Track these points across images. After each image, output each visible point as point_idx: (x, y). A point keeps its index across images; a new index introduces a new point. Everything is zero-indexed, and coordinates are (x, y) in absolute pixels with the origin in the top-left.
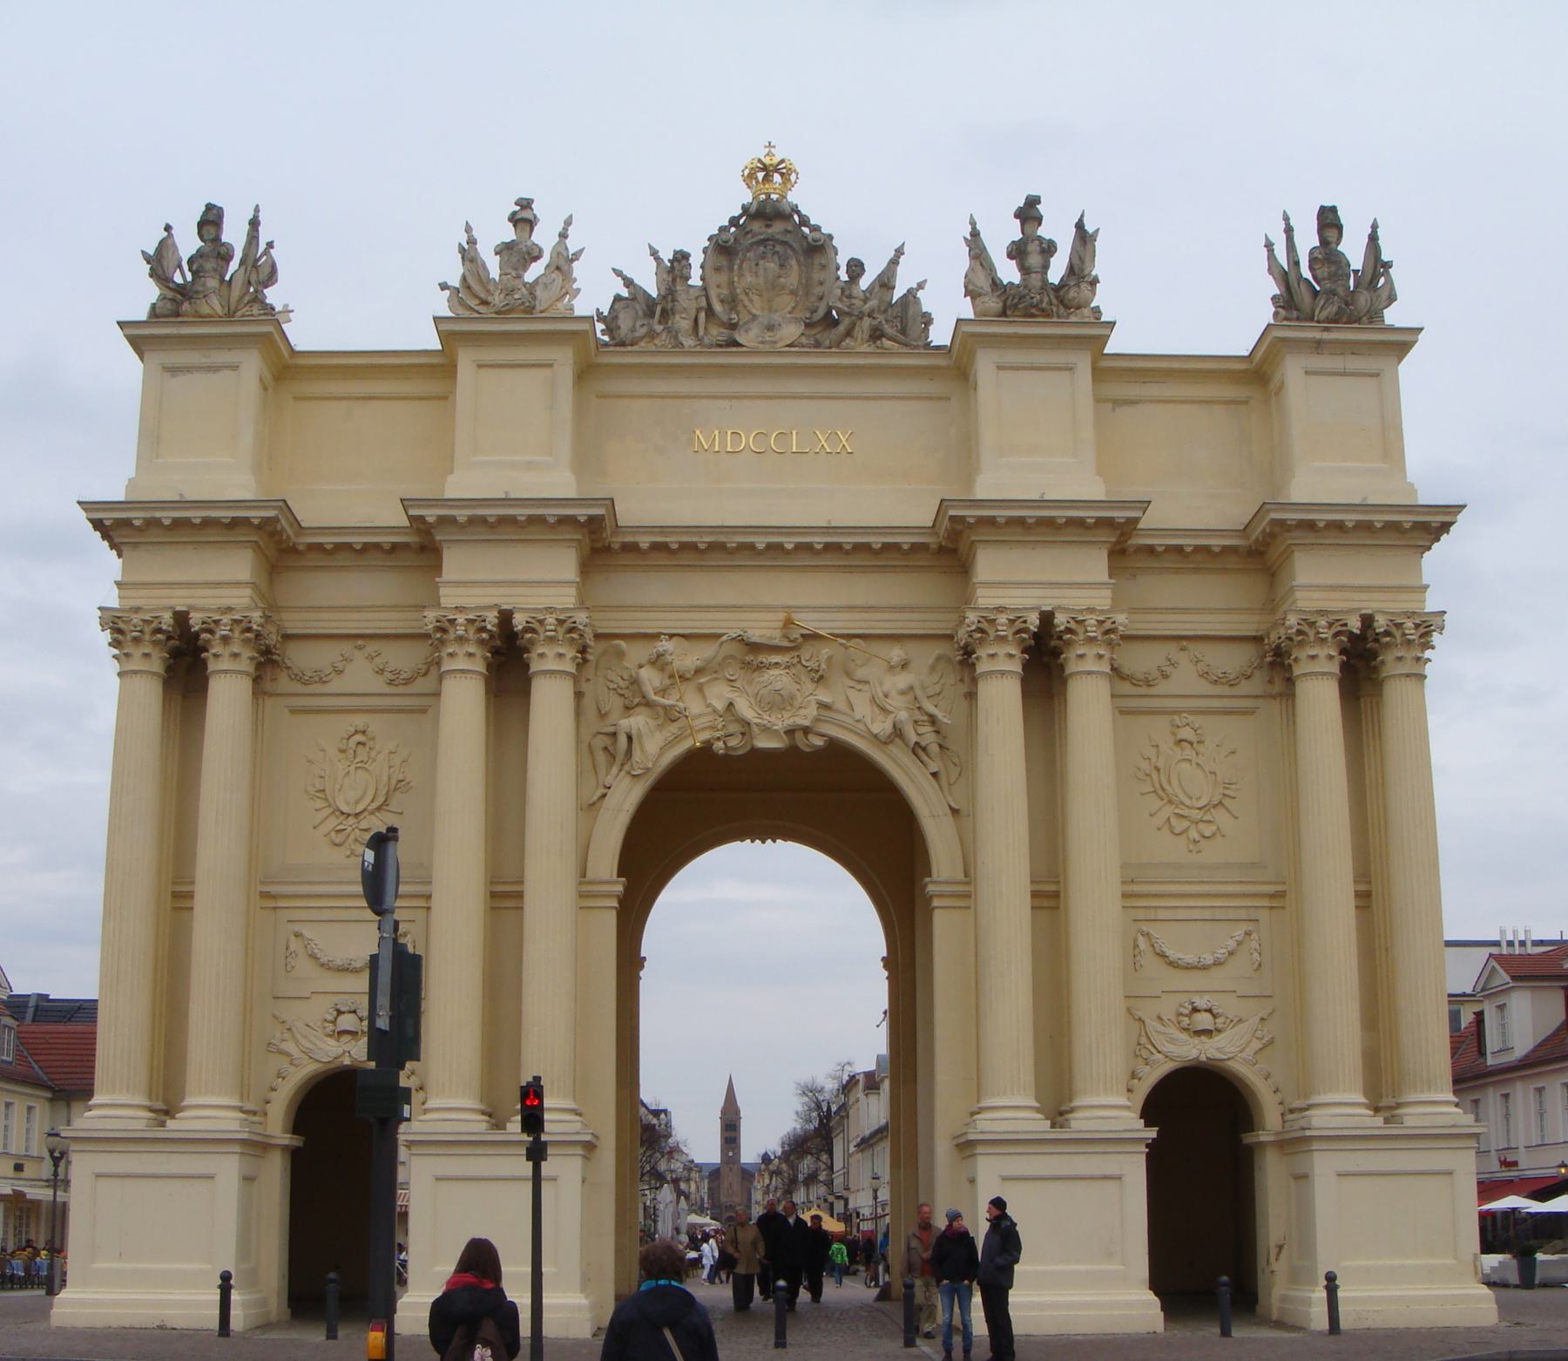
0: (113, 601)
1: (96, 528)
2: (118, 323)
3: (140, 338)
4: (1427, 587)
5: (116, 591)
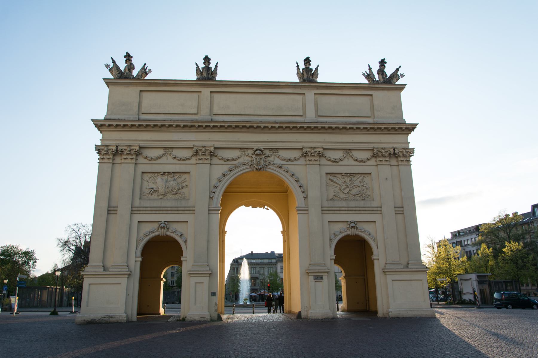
0: (99, 143)
2: (103, 79)
3: (108, 82)
4: (410, 143)
5: (100, 141)
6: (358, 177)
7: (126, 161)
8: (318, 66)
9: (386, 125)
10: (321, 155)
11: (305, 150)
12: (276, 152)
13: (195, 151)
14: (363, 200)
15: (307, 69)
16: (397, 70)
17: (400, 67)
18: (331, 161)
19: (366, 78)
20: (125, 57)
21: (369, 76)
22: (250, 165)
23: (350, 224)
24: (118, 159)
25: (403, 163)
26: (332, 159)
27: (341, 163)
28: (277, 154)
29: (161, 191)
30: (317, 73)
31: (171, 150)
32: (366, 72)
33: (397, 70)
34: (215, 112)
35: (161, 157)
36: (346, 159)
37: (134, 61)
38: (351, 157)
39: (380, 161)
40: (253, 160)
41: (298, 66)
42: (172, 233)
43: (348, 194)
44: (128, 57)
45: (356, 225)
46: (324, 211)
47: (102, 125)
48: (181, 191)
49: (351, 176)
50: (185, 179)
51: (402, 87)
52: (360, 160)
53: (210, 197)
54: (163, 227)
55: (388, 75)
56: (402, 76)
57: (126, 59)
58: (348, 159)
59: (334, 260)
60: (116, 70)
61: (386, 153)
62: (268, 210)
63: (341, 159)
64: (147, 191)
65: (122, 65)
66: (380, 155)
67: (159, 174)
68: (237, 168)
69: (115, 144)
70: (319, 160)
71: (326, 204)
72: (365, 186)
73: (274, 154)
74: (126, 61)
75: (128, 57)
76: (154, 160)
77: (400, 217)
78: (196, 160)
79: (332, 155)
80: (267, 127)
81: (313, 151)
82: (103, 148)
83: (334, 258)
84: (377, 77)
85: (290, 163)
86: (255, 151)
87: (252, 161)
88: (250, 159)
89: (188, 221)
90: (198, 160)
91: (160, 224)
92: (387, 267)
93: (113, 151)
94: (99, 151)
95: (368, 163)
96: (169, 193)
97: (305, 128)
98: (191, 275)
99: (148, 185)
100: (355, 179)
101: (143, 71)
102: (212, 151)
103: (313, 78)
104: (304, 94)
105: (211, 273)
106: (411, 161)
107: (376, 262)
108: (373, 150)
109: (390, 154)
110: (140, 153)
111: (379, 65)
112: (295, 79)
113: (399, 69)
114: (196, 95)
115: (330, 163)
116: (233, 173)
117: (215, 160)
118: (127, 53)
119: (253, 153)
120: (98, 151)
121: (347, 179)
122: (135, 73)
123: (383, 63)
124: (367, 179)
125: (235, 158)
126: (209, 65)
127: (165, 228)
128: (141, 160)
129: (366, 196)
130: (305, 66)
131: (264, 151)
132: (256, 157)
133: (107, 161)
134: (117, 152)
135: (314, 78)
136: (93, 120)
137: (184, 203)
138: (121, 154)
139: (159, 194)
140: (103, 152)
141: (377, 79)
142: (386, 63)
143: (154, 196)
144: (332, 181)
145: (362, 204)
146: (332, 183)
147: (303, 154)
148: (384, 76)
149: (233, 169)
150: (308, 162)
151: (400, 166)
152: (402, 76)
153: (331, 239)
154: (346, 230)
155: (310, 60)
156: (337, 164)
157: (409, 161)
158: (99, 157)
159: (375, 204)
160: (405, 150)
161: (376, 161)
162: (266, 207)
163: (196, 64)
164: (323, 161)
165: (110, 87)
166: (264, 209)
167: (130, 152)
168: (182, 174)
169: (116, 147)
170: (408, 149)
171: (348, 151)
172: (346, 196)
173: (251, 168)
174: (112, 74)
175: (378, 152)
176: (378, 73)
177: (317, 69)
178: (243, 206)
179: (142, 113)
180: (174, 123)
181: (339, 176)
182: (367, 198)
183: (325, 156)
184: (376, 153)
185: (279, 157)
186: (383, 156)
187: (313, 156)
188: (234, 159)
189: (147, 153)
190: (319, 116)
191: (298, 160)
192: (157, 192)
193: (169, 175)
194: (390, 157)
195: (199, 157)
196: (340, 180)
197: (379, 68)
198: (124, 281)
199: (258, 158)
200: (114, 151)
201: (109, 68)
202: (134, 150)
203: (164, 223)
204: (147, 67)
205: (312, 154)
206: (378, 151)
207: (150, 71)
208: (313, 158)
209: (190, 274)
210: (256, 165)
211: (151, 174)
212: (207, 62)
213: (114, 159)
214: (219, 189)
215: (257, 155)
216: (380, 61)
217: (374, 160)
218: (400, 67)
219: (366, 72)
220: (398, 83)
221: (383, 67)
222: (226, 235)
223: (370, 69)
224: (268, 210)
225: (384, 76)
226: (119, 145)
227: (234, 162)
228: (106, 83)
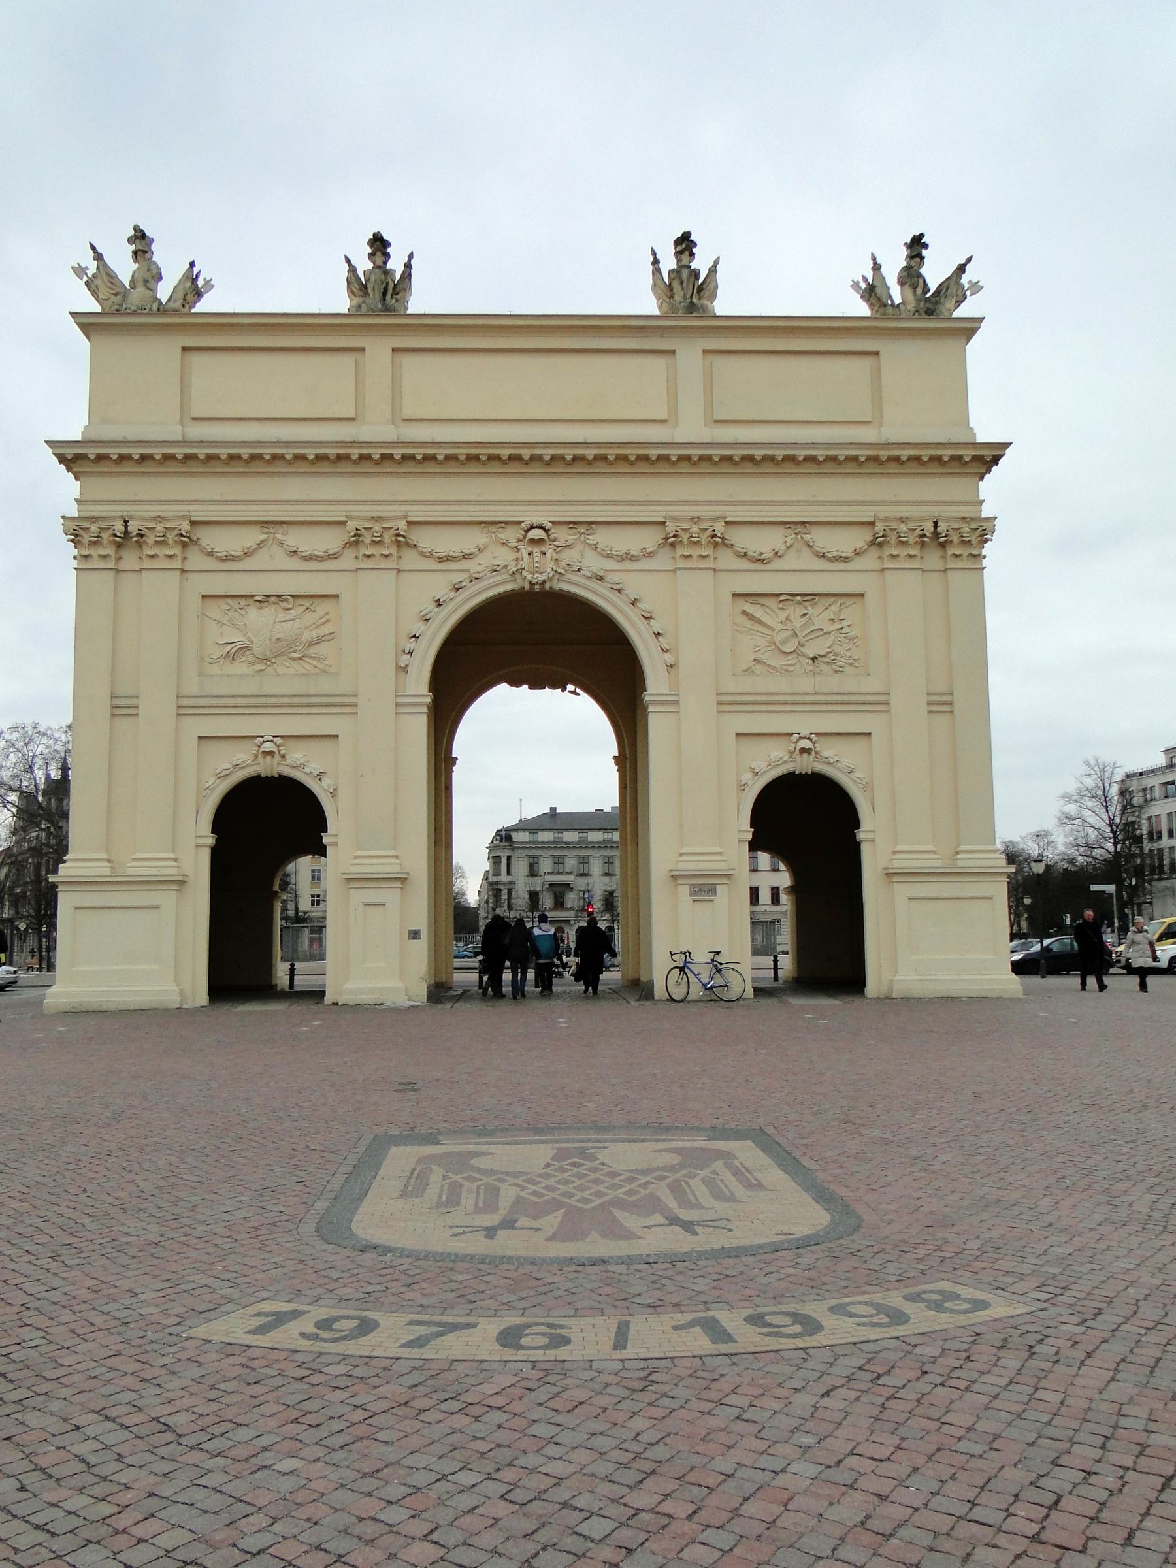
0: (73, 511)
1: (61, 462)
2: (71, 313)
3: (87, 324)
4: (983, 501)
6: (827, 605)
7: (156, 564)
8: (717, 262)
9: (913, 449)
10: (717, 539)
11: (671, 527)
12: (588, 532)
13: (353, 534)
14: (836, 672)
16: (961, 269)
17: (969, 260)
18: (749, 559)
19: (862, 297)
20: (131, 240)
21: (872, 292)
22: (513, 573)
23: (798, 741)
24: (130, 559)
25: (960, 564)
26: (750, 553)
27: (777, 564)
28: (592, 540)
29: (258, 650)
30: (712, 285)
31: (281, 530)
32: (865, 279)
33: (961, 269)
34: (408, 412)
35: (255, 550)
36: (792, 552)
37: (160, 254)
38: (809, 545)
39: (893, 556)
40: (520, 556)
41: (656, 262)
42: (295, 767)
43: (795, 655)
44: (141, 240)
45: (814, 743)
46: (727, 704)
47: (78, 458)
48: (312, 651)
49: (805, 604)
50: (327, 614)
51: (969, 329)
52: (835, 554)
53: (398, 667)
54: (271, 753)
55: (933, 287)
56: (976, 288)
57: (133, 247)
58: (798, 551)
59: (750, 842)
60: (109, 284)
61: (911, 533)
62: (579, 694)
63: (777, 553)
64: (218, 652)
65: (124, 267)
66: (893, 539)
67: (250, 601)
68: (475, 581)
69: (119, 514)
70: (711, 554)
71: (731, 685)
72: (844, 631)
73: (583, 537)
74: (135, 253)
75: (141, 240)
76: (235, 558)
77: (942, 721)
78: (357, 558)
80: (562, 458)
81: (695, 529)
82: (86, 525)
83: (750, 836)
85: (627, 565)
86: (527, 531)
87: (517, 559)
88: (515, 555)
89: (337, 736)
90: (360, 558)
91: (262, 744)
92: (896, 864)
93: (115, 535)
94: (76, 536)
95: (857, 564)
96: (281, 655)
97: (674, 458)
98: (352, 885)
99: (222, 634)
100: (819, 609)
101: (189, 284)
102: (402, 533)
103: (700, 299)
104: (673, 352)
105: (406, 879)
106: (985, 557)
107: (866, 851)
108: (872, 524)
109: (924, 536)
110: (194, 538)
111: (904, 252)
112: (647, 304)
113: (968, 267)
114: (348, 360)
115: (744, 564)
116: (463, 594)
117: (410, 559)
118: (137, 229)
119: (521, 537)
120: (71, 534)
121: (794, 612)
122: (164, 291)
123: (917, 245)
124: (851, 613)
125: (467, 552)
126: (385, 263)
127: (277, 755)
128: (196, 560)
129: (848, 661)
130: (679, 261)
131: (553, 531)
132: (530, 549)
133: (96, 563)
134: (127, 539)
135: (705, 302)
136: (50, 443)
137: (325, 685)
138: (140, 545)
139: (254, 658)
140: (86, 539)
141: (898, 300)
142: (926, 246)
143: (239, 668)
144: (751, 617)
145: (833, 683)
146: (749, 624)
147: (668, 538)
148: (919, 291)
149: (464, 584)
150: (681, 563)
151: (948, 571)
152: (976, 288)
153: (743, 783)
154: (786, 758)
155: (692, 241)
156: (768, 567)
157: (978, 557)
158: (75, 552)
159: (872, 684)
160: (967, 522)
161: (880, 557)
162: (570, 687)
163: (348, 261)
164: (725, 559)
165: (91, 337)
166: (566, 692)
167: (164, 536)
168: (317, 601)
169: (123, 523)
170: (980, 520)
171: (799, 528)
172: (791, 660)
173: (515, 580)
174: (94, 293)
175: (889, 531)
176: (902, 282)
177: (713, 271)
178: (504, 687)
179: (194, 419)
180: (287, 447)
181: (772, 603)
182: (848, 669)
183: (732, 542)
184: (881, 534)
185: (595, 547)
186: (902, 543)
187: (695, 543)
188: (465, 556)
189: (210, 539)
190: (716, 421)
191: (650, 555)
192: (248, 653)
193: (281, 603)
194: (923, 545)
195: (364, 551)
196: (771, 615)
197: (905, 264)
198: (167, 899)
199: (536, 551)
200: (118, 534)
201: (85, 279)
202: (176, 532)
203: (272, 741)
204: (199, 272)
205: (692, 537)
206: (886, 528)
208: (695, 552)
209: (348, 880)
210: (530, 573)
211: (229, 600)
212: (379, 253)
213: (119, 559)
214: (423, 641)
215: (533, 542)
216: (909, 241)
217: (874, 552)
218: (969, 260)
219: (863, 277)
220: (961, 312)
221: (918, 260)
222: (454, 768)
223: (876, 267)
224: (579, 694)
225: (919, 291)
226: (132, 518)
227: (465, 564)
228: (79, 324)
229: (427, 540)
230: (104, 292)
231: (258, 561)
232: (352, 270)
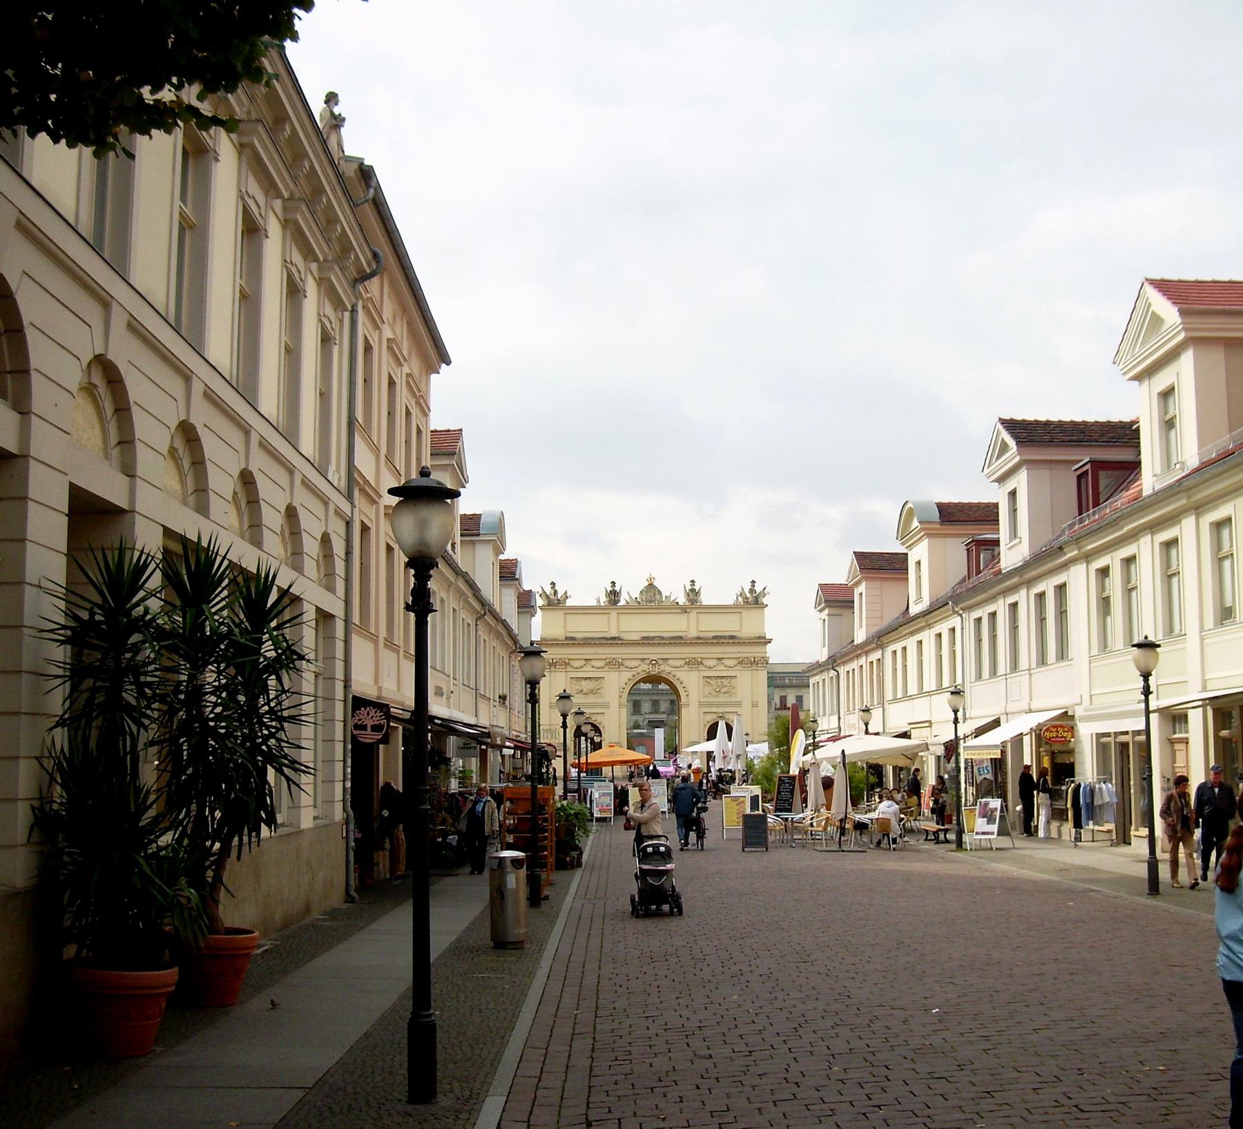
15: (693, 590)
16: (765, 589)
29: (584, 691)
33: (765, 589)
44: (553, 584)
46: (701, 705)
65: (549, 591)
75: (553, 584)
79: (707, 663)
84: (748, 595)
95: (735, 668)
114: (606, 616)
117: (622, 668)
121: (719, 680)
124: (733, 681)
128: (569, 669)
137: (601, 700)
143: (580, 696)
164: (702, 668)
207: (570, 597)
229: (627, 663)
230: (544, 598)
231: (585, 668)
232: (606, 591)
